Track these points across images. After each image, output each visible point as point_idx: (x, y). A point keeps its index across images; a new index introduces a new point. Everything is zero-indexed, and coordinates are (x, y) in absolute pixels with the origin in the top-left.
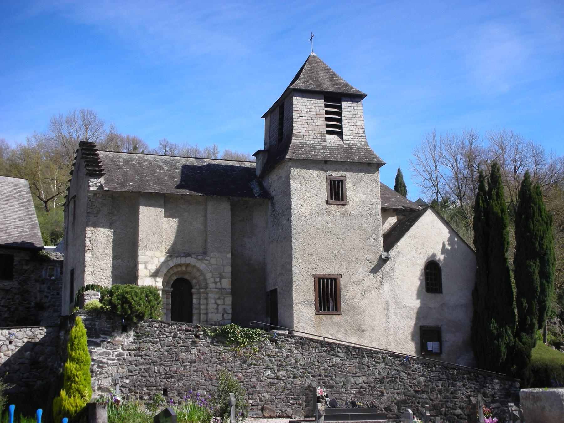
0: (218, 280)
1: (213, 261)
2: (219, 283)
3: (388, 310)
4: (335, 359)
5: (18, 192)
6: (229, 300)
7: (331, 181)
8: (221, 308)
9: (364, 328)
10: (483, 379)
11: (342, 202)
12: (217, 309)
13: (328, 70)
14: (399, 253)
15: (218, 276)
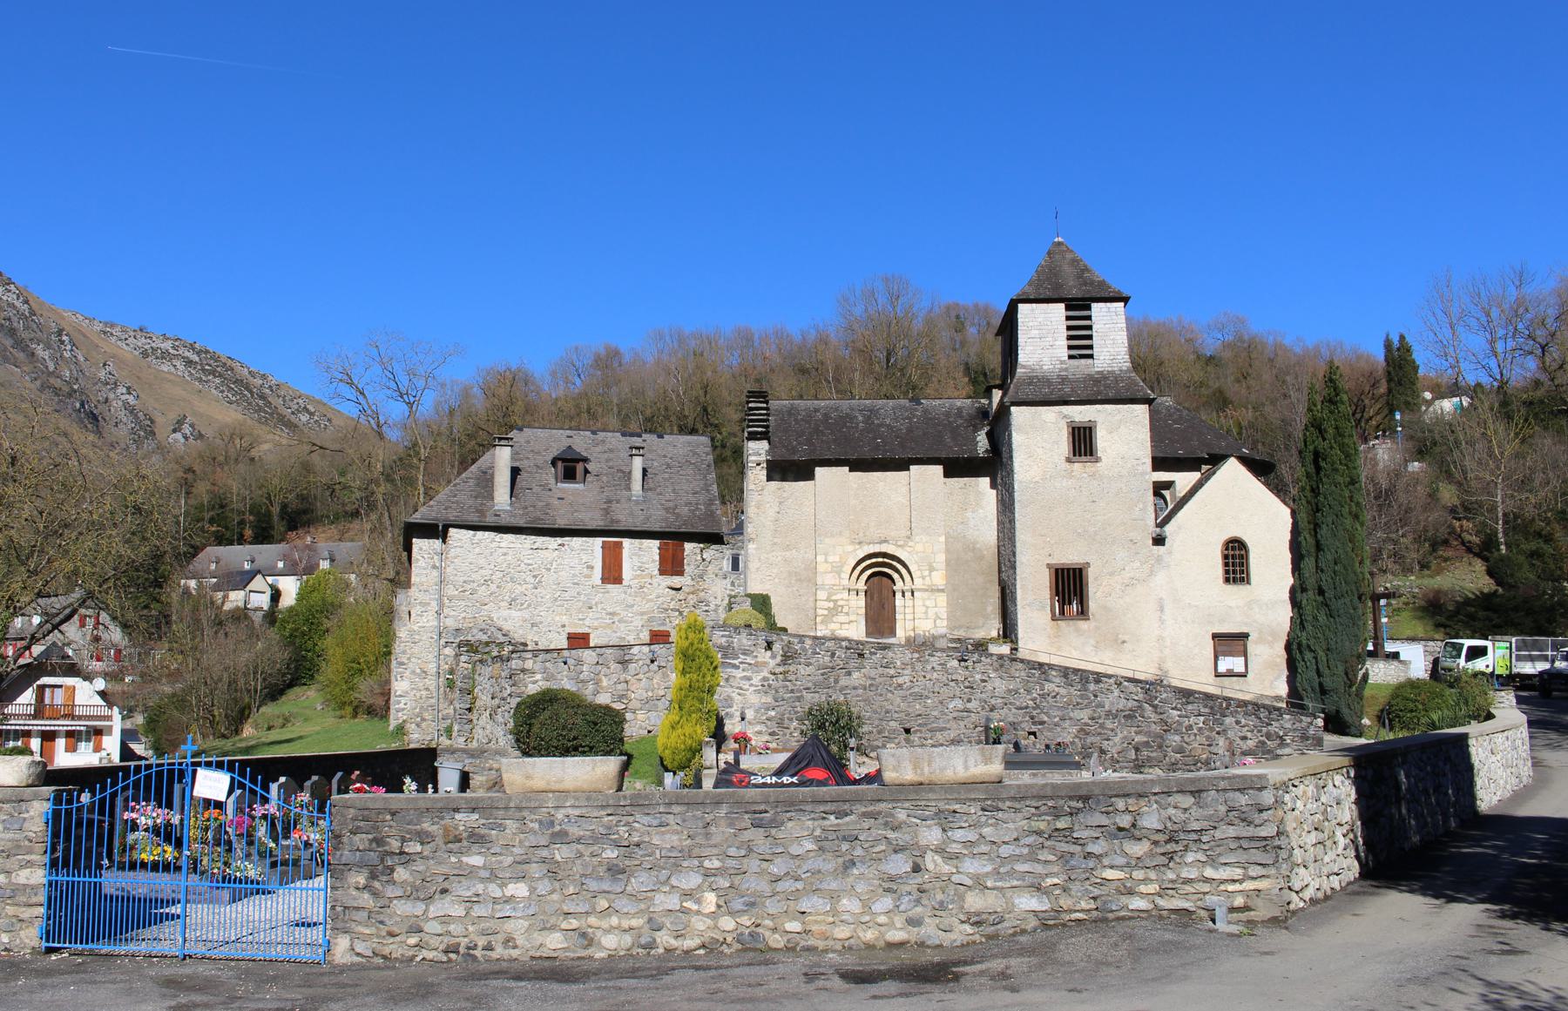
1: (919, 547)
3: (1162, 610)
4: (1048, 687)
5: (695, 454)
6: (942, 599)
8: (931, 613)
9: (1126, 638)
13: (1075, 262)
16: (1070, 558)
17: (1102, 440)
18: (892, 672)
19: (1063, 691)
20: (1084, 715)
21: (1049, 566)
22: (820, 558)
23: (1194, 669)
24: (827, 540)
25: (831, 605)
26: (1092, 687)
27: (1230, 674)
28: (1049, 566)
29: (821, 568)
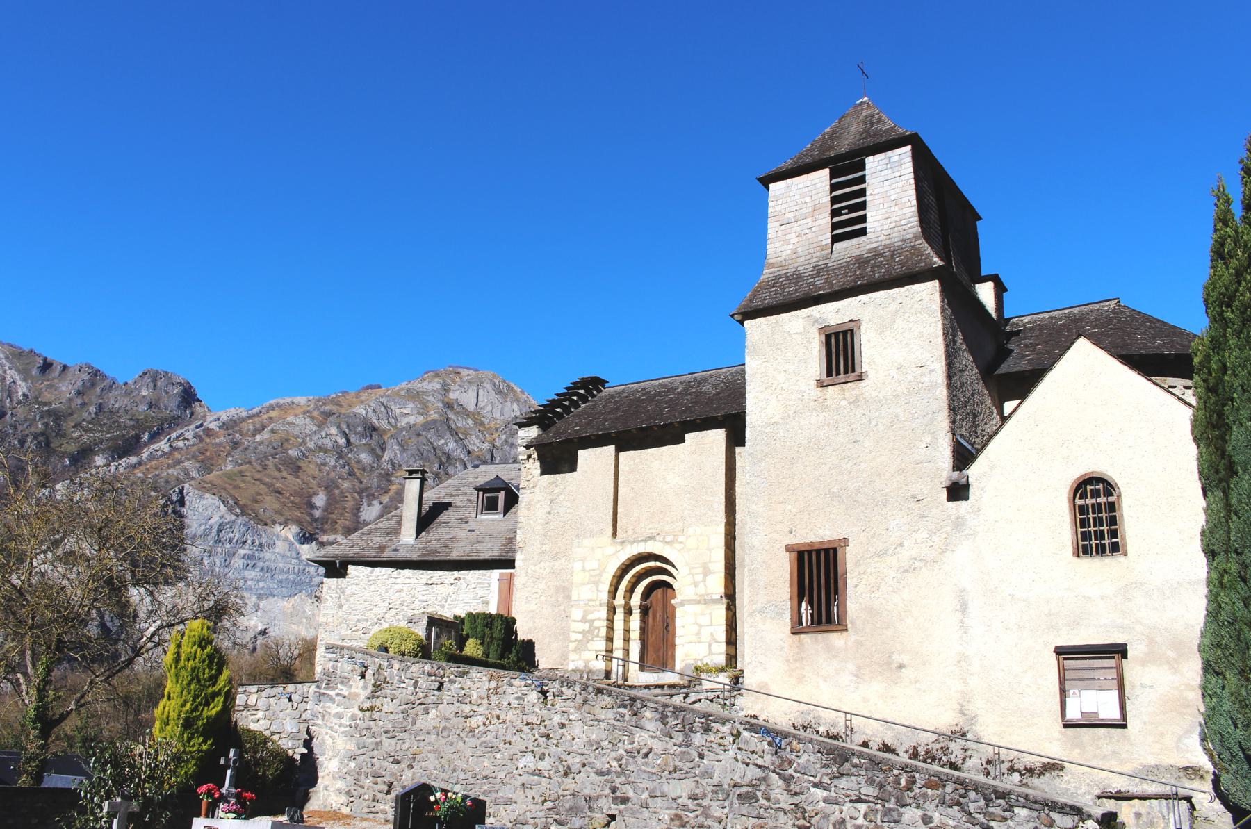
0: (699, 578)
2: (701, 585)
3: (964, 608)
7: (828, 337)
9: (905, 659)
10: (982, 802)
11: (851, 376)
12: (698, 634)
14: (992, 468)
15: (700, 570)
16: (816, 533)
17: (869, 349)
18: (467, 709)
19: (657, 746)
20: (681, 789)
21: (789, 548)
22: (578, 566)
23: (1019, 718)
24: (586, 542)
25: (586, 626)
26: (698, 739)
27: (1091, 723)
28: (789, 548)
29: (579, 577)
